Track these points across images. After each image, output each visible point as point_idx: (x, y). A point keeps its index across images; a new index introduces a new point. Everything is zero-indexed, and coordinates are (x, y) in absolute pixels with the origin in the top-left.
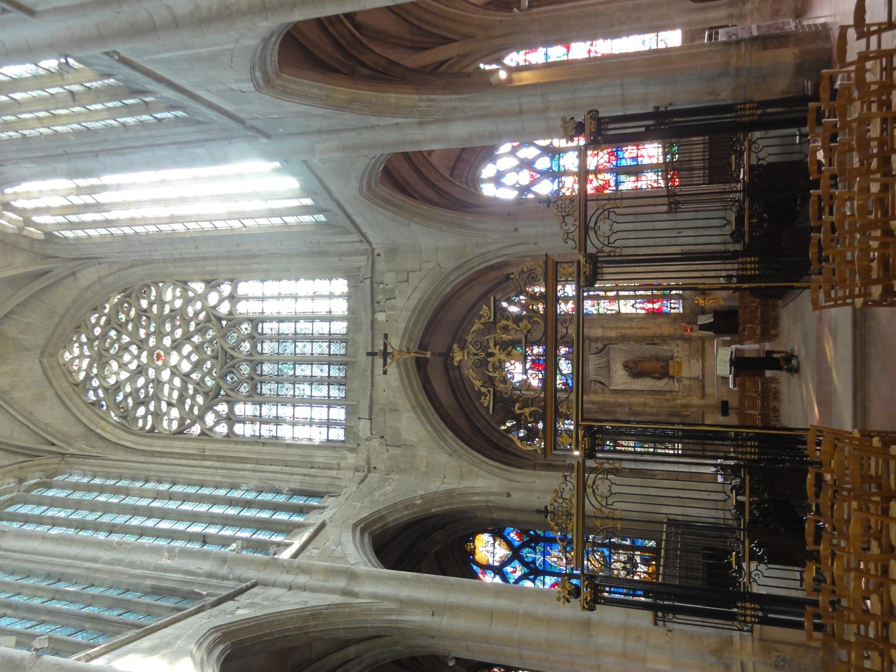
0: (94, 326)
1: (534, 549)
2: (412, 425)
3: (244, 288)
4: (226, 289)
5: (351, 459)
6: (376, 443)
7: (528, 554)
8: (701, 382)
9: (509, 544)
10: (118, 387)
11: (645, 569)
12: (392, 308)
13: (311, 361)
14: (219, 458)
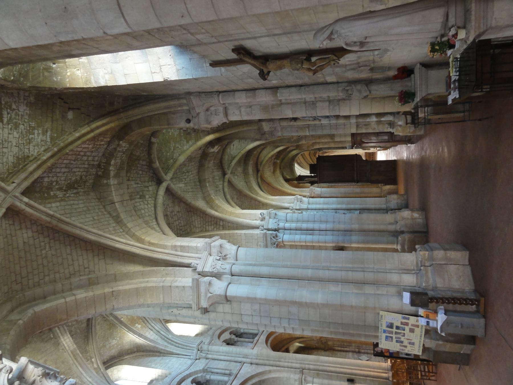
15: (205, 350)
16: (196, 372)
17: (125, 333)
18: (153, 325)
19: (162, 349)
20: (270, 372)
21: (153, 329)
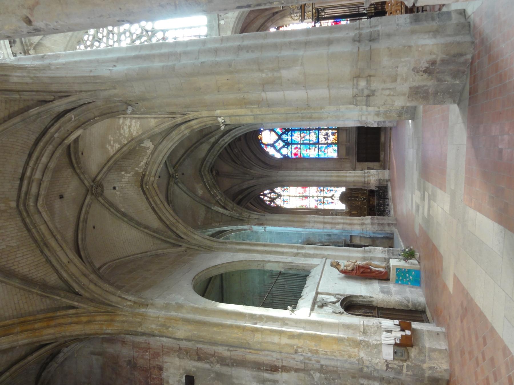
0: (86, 41)
1: (287, 134)
7: (284, 137)
9: (277, 134)
11: (333, 137)
12: (227, 18)
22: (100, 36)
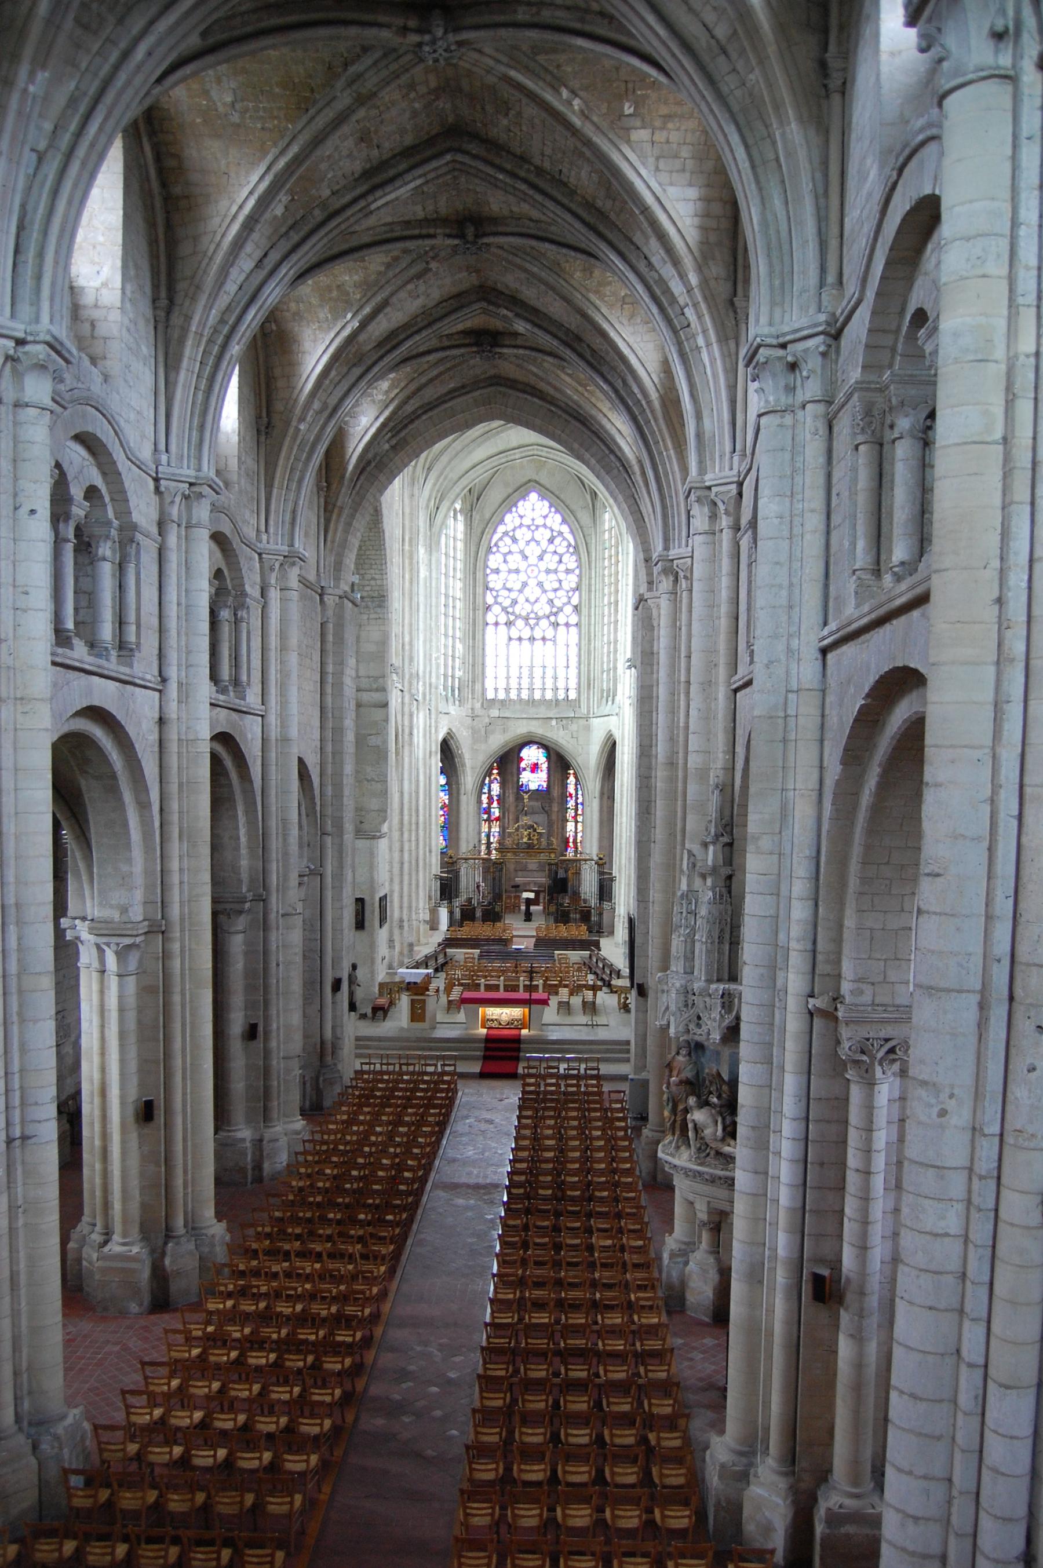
2: (497, 742)
3: (573, 630)
4: (574, 619)
5: (478, 705)
6: (487, 720)
8: (525, 869)
10: (515, 540)
13: (531, 677)
14: (474, 620)
15: (189, 509)
16: (120, 496)
17: (264, 153)
18: (283, 270)
19: (188, 318)
20: (143, 805)
21: (264, 273)
22: (557, 541)
